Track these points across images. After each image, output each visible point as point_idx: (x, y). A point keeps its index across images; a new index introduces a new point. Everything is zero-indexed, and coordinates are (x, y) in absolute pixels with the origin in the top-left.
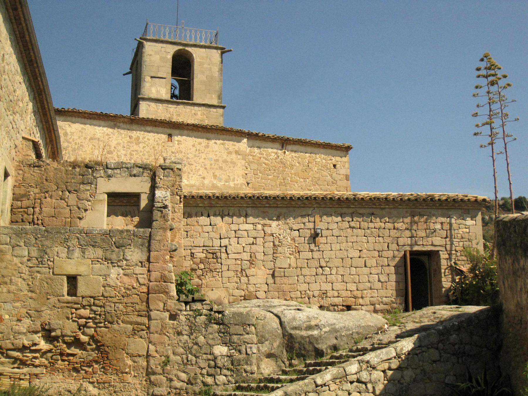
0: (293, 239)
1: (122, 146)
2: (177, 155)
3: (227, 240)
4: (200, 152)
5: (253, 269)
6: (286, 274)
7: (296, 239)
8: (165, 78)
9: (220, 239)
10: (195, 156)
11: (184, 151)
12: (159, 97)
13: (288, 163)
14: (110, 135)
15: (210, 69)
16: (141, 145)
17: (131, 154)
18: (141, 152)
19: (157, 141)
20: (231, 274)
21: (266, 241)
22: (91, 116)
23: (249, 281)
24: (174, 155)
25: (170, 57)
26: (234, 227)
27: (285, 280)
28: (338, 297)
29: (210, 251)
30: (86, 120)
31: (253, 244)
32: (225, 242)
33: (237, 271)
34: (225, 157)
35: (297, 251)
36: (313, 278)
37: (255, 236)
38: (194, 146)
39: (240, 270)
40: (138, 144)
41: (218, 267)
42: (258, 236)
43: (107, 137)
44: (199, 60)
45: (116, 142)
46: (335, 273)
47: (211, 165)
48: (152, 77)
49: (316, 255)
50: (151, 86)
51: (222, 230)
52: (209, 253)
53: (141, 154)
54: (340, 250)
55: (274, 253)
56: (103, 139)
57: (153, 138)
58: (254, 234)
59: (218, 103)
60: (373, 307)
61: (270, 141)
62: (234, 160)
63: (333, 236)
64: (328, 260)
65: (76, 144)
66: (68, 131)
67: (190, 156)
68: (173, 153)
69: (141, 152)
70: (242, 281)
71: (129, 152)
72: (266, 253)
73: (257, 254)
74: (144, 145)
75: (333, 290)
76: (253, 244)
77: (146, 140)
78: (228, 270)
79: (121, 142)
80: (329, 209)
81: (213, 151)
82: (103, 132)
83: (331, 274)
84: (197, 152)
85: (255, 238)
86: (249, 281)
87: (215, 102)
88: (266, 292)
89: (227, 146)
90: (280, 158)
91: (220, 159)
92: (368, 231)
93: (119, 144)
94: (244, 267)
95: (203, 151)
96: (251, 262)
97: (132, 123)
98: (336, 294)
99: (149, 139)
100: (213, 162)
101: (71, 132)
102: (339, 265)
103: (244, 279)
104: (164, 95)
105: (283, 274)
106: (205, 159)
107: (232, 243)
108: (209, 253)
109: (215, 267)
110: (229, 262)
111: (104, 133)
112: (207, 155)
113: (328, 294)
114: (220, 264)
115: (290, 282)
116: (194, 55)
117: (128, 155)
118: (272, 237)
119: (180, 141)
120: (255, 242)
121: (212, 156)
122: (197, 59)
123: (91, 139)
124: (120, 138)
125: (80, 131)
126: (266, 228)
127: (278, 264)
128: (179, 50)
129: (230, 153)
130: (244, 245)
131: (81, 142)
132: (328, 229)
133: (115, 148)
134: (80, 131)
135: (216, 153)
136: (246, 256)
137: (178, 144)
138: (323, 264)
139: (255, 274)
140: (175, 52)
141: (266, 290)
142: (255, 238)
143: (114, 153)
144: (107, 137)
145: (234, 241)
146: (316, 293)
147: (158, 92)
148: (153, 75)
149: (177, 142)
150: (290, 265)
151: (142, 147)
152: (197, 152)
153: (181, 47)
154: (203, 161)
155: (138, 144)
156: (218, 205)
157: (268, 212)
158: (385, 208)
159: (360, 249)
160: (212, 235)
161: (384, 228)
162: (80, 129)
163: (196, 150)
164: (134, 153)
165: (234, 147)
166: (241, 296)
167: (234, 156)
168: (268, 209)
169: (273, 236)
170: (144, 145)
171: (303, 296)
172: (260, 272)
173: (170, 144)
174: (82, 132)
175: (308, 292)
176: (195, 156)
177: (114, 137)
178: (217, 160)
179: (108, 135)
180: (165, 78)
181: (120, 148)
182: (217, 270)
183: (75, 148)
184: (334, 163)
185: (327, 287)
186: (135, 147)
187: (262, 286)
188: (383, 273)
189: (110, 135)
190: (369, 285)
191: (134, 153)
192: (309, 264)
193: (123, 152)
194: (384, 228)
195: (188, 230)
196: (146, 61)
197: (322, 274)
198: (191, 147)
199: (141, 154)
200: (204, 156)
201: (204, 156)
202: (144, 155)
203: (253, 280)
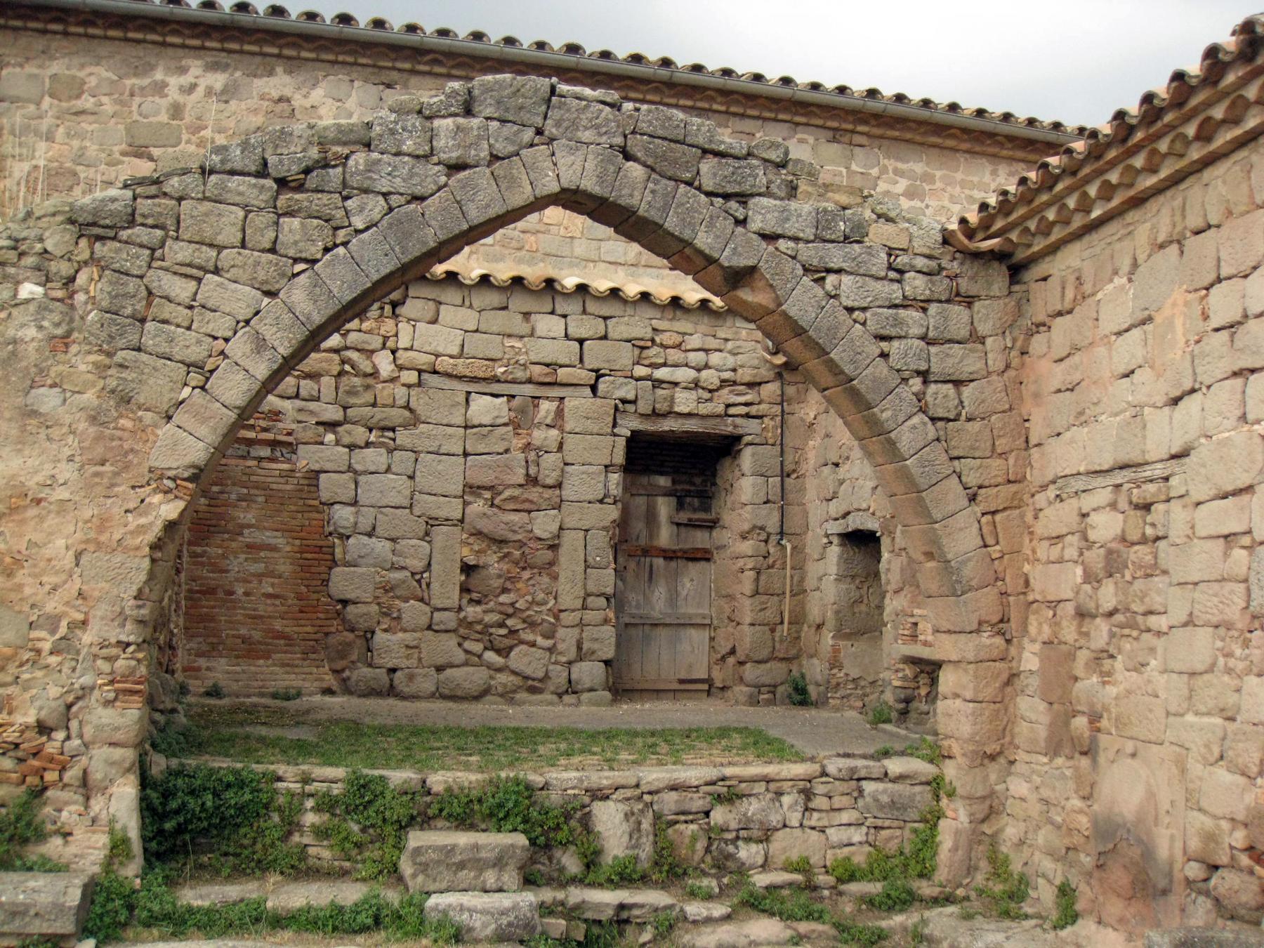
20: (1201, 645)
33: (1229, 626)
156: (1150, 181)
182: (1153, 621)
195: (1077, 377)
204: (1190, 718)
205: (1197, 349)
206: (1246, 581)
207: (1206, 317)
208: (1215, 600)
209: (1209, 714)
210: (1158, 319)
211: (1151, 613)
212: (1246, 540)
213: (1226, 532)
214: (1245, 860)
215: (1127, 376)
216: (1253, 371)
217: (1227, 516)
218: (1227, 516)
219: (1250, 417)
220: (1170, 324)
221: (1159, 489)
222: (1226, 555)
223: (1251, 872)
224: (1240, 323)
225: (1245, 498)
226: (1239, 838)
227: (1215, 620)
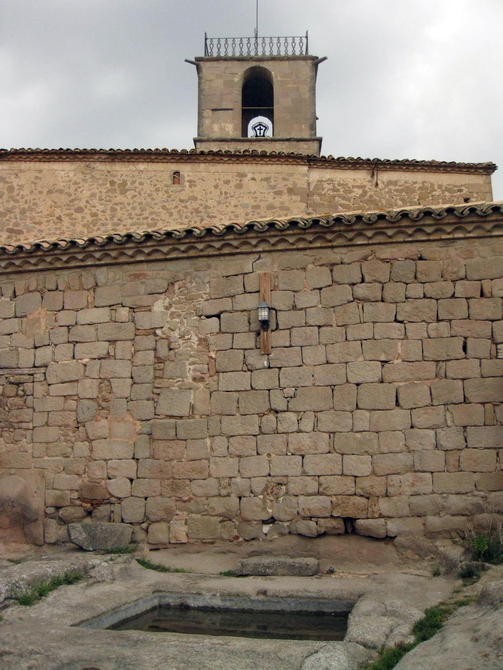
0: (203, 341)
1: (97, 198)
2: (188, 204)
3: (48, 351)
4: (228, 195)
5: (104, 422)
6: (182, 434)
7: (212, 339)
8: (231, 109)
9: (36, 348)
10: (219, 203)
11: (199, 197)
12: (224, 136)
13: (384, 202)
14: (79, 183)
15: (298, 89)
16: (129, 194)
17: (113, 210)
18: (129, 204)
19: (155, 185)
20: (53, 433)
21: (138, 348)
22: (48, 157)
23: (91, 450)
24: (183, 204)
25: (238, 80)
26: (65, 318)
27: (176, 448)
28: (319, 493)
29: (12, 379)
30: (42, 164)
31: (108, 356)
32: (44, 355)
33: (66, 426)
34: (271, 200)
35: (213, 372)
36: (251, 443)
37: (114, 337)
38: (216, 187)
39: (73, 424)
40: (124, 192)
41: (27, 418)
42: (121, 336)
43: (73, 187)
44: (279, 79)
45: (89, 193)
46: (309, 428)
47: (247, 214)
48: (213, 110)
49: (262, 380)
50: (213, 122)
51: (39, 328)
52: (11, 383)
53: (129, 208)
54: (328, 363)
55: (155, 377)
56: (66, 190)
57: (148, 181)
58: (109, 331)
59: (311, 135)
60: (420, 521)
61: (350, 169)
62: (287, 204)
63: (307, 325)
64: (290, 391)
65: (26, 202)
66: (15, 184)
67: (210, 203)
68: (181, 201)
69: (129, 204)
70: (77, 451)
71: (109, 207)
72: (137, 380)
73: (115, 383)
74: (134, 193)
75: (304, 474)
76: (108, 356)
77: (137, 184)
78: (47, 424)
79: (97, 191)
80: (298, 255)
81: (250, 193)
82: (68, 179)
83: (299, 431)
84: (223, 196)
85: (112, 342)
86: (91, 450)
87: (306, 136)
88: (131, 480)
89: (273, 183)
90: (368, 194)
91: (263, 205)
92: (407, 307)
93: (93, 195)
94: (81, 418)
95: (232, 194)
96: (103, 404)
97: (113, 161)
98: (313, 486)
99: (141, 184)
100: (250, 210)
101: (18, 185)
102: (322, 405)
103: (82, 448)
104: (231, 133)
105: (172, 433)
106: (235, 206)
107: (58, 357)
108: (11, 383)
109: (20, 418)
110: (51, 404)
111: (70, 181)
112: (240, 199)
113: (291, 486)
114: (31, 410)
115: (193, 454)
116: (273, 73)
117: (108, 212)
118: (152, 337)
119: (195, 182)
120: (112, 353)
121: (248, 201)
122: (276, 77)
123: (50, 192)
124: (95, 186)
125: (33, 182)
126: (139, 315)
127: (164, 408)
128: (253, 69)
129: (279, 193)
130: (86, 360)
131: (34, 199)
132: (294, 308)
133: (87, 202)
134: (33, 182)
135: (255, 195)
136: (89, 388)
137: (190, 186)
138: (279, 403)
139: (106, 432)
140: (246, 71)
141: (133, 475)
142: (112, 342)
143: (86, 211)
144: (73, 187)
145: (65, 350)
146: (259, 485)
147: (222, 129)
148: (214, 107)
149: (187, 184)
150: (192, 407)
151: (130, 197)
152: (223, 196)
153: (254, 64)
154: (233, 209)
155: (124, 192)
157: (145, 275)
158: (454, 239)
159: (383, 358)
160: (19, 339)
161: (453, 296)
162: (33, 179)
163: (221, 193)
164: (118, 208)
165: (286, 183)
166: (72, 490)
167: (285, 197)
168: (145, 266)
169: (155, 334)
170: (134, 193)
171: (224, 492)
172: (120, 428)
173: (176, 187)
174: (35, 184)
175: (238, 480)
176: (219, 203)
177: (86, 185)
178: (258, 207)
179: (76, 183)
180: (231, 109)
181: (96, 202)
182: (24, 425)
183: (24, 209)
184: (466, 197)
185: (290, 466)
186: (120, 198)
187: (123, 463)
188: (449, 423)
189: (79, 183)
190: (404, 459)
191: (118, 208)
192: (242, 405)
193: (101, 208)
194: (453, 296)
196: (204, 89)
197: (276, 432)
198: (213, 189)
199: (129, 208)
200: (233, 202)
201: (233, 202)
202: (134, 208)
203: (101, 449)
204: (46, 458)
205: (51, 331)
206: (76, 411)
207: (56, 321)
208: (60, 417)
209: (57, 456)
210: (30, 317)
211: (21, 422)
212: (76, 398)
213: (66, 394)
214: (78, 502)
215: (9, 335)
216: (77, 342)
217: (68, 389)
218: (68, 389)
219: (76, 357)
220: (38, 320)
221: (30, 378)
222: (65, 403)
223: (81, 506)
224: (73, 326)
225: (76, 384)
226: (75, 495)
227: (60, 424)
